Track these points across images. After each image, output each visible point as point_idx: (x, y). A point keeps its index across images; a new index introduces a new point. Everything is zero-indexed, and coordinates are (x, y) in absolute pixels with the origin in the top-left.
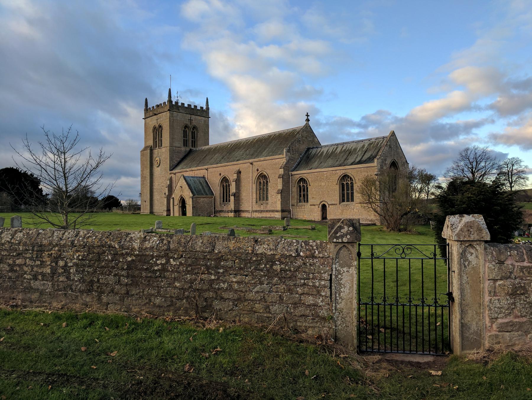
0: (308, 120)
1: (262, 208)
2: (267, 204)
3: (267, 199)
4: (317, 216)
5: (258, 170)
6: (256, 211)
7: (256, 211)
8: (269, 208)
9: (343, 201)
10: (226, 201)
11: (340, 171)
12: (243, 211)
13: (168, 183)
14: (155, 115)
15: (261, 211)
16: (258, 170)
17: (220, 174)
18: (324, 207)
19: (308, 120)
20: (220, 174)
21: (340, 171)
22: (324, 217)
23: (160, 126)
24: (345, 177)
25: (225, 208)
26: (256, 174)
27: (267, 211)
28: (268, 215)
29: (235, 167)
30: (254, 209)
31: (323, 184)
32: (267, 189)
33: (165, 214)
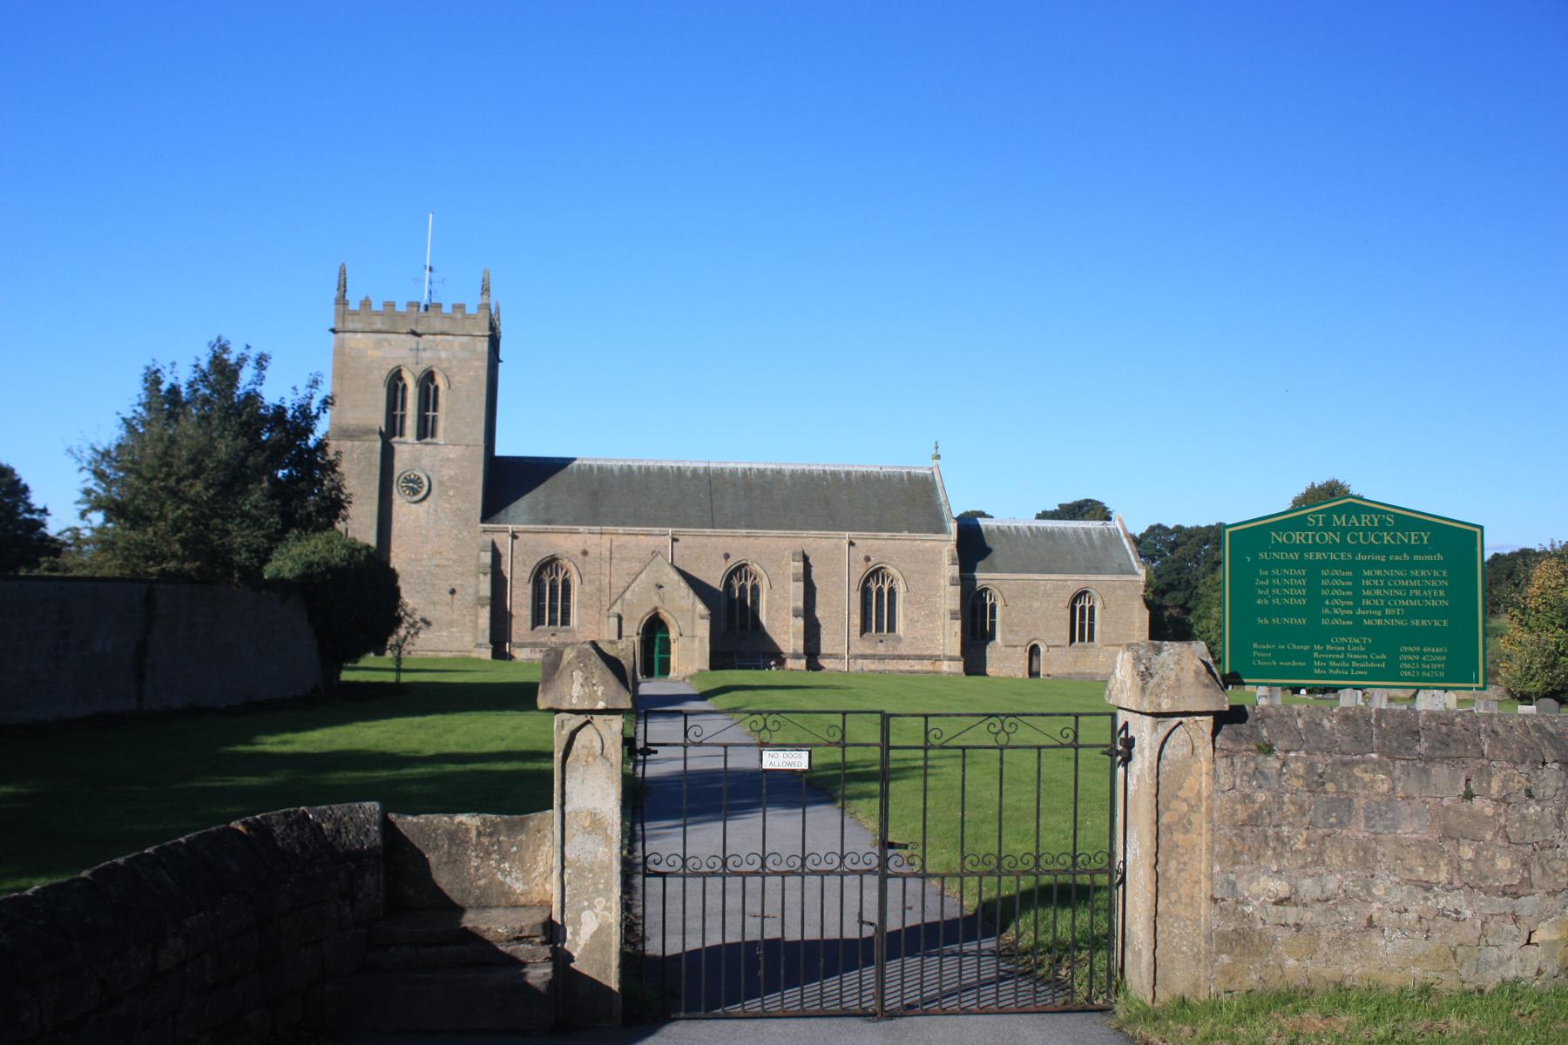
1: (881, 649)
2: (899, 639)
3: (892, 628)
5: (868, 559)
6: (864, 657)
7: (864, 657)
8: (903, 650)
11: (1075, 582)
13: (487, 558)
15: (882, 658)
16: (868, 559)
17: (727, 556)
18: (1034, 651)
20: (727, 556)
21: (1075, 582)
22: (1033, 674)
26: (860, 570)
27: (901, 657)
28: (904, 666)
29: (787, 542)
30: (853, 651)
31: (1036, 604)
33: (486, 654)
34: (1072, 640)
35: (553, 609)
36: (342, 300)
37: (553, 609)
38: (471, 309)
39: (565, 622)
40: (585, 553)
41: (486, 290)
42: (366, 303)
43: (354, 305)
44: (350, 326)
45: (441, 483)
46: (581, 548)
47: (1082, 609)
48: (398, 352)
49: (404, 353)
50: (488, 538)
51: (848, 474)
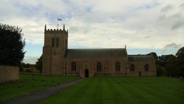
0: (126, 47)
1: (118, 73)
2: (120, 72)
3: (120, 70)
4: (138, 75)
5: (116, 61)
6: (116, 74)
9: (145, 71)
10: (99, 70)
12: (110, 74)
13: (65, 62)
14: (54, 33)
16: (116, 61)
17: (97, 61)
18: (140, 73)
19: (126, 47)
20: (97, 61)
23: (57, 38)
24: (147, 65)
25: (99, 73)
28: (121, 75)
32: (119, 67)
34: (145, 71)
35: (74, 69)
36: (45, 29)
37: (74, 69)
38: (62, 30)
39: (75, 70)
40: (78, 61)
41: (64, 27)
42: (49, 30)
43: (47, 30)
44: (47, 32)
45: (59, 52)
46: (77, 60)
47: (146, 67)
48: (53, 35)
49: (54, 36)
50: (65, 60)
51: (114, 50)
